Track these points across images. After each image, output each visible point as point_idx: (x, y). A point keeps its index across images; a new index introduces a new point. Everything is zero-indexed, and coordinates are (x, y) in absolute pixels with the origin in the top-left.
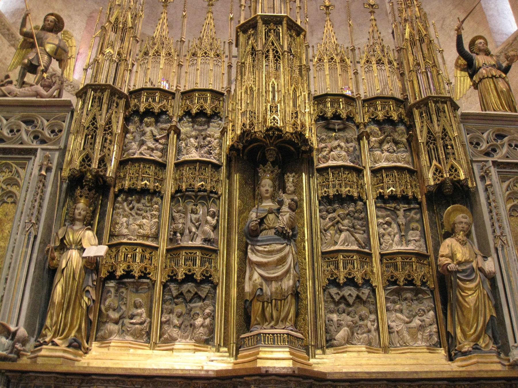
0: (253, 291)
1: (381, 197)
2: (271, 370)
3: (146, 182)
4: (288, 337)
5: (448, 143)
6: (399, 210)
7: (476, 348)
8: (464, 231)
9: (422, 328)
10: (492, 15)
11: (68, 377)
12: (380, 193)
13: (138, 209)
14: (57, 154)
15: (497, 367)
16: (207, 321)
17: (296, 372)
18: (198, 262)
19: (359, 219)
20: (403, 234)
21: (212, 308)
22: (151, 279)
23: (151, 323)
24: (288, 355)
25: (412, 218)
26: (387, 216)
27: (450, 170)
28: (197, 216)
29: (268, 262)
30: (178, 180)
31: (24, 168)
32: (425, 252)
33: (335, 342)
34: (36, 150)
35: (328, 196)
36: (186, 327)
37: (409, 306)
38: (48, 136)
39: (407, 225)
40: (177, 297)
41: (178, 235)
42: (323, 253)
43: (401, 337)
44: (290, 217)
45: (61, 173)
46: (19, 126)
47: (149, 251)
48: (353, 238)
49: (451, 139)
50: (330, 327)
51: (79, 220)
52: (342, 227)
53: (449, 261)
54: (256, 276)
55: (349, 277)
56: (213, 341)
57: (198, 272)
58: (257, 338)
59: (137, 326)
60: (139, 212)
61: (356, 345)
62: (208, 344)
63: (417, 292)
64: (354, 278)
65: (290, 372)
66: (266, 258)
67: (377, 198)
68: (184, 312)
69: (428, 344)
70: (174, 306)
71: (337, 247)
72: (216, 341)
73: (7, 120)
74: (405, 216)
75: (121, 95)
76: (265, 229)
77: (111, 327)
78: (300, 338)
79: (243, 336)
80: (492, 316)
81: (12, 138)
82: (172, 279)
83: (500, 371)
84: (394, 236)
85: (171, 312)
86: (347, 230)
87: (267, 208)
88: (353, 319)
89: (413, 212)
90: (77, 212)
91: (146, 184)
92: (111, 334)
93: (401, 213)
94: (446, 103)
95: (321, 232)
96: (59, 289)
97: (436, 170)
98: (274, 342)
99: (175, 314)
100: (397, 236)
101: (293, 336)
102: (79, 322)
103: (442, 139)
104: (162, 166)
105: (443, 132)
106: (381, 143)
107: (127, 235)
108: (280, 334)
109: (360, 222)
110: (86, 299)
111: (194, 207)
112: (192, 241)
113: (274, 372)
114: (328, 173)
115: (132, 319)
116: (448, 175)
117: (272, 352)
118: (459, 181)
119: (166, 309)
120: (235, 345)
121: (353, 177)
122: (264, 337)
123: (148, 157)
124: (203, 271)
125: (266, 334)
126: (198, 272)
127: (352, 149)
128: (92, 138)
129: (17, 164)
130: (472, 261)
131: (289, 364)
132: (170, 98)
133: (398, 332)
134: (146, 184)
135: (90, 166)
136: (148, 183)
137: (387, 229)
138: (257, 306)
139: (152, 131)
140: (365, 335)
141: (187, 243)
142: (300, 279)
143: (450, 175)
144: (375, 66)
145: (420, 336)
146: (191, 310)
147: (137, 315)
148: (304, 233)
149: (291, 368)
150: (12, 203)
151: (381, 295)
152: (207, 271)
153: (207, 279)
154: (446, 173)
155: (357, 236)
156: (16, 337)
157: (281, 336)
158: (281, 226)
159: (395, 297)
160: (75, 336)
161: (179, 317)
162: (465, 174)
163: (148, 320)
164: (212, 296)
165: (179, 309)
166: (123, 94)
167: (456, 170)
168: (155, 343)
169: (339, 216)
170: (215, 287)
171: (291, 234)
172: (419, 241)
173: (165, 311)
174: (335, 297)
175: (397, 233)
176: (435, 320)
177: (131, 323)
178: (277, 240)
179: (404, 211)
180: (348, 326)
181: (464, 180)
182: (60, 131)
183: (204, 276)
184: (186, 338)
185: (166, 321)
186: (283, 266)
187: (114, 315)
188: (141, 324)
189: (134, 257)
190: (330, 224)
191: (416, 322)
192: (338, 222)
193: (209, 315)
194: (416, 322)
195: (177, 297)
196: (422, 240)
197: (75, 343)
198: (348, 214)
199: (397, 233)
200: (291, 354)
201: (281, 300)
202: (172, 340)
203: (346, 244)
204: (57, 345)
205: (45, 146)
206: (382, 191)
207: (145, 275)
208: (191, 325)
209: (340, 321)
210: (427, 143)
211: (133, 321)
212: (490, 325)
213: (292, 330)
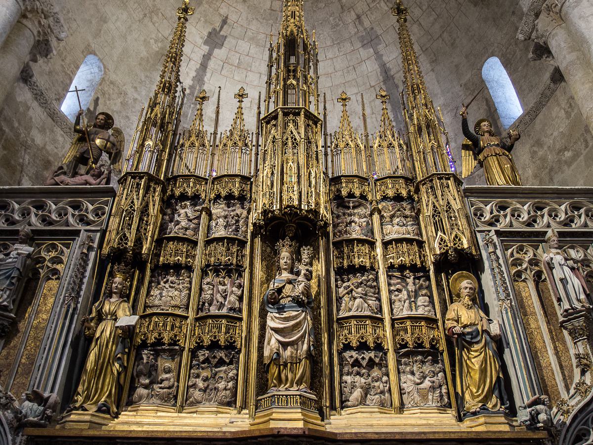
0: (270, 355)
2: (282, 430)
3: (179, 257)
4: (300, 398)
5: (452, 215)
6: (409, 278)
7: (484, 409)
8: (469, 296)
9: (433, 388)
10: (500, 102)
11: (94, 441)
12: (391, 263)
13: (172, 283)
14: (99, 234)
15: (506, 428)
16: (230, 385)
17: (307, 433)
18: (223, 329)
19: (371, 287)
20: (413, 299)
21: (235, 371)
22: (180, 346)
23: (178, 386)
24: (299, 416)
25: (422, 285)
26: (398, 284)
27: (454, 239)
28: (224, 288)
29: (285, 328)
31: (68, 248)
32: (434, 317)
33: (349, 403)
34: (80, 231)
35: (343, 266)
36: (211, 390)
37: (419, 367)
38: (93, 219)
40: (203, 362)
41: (206, 304)
42: (338, 319)
43: (412, 397)
44: (305, 286)
45: (100, 252)
46: (66, 209)
47: (179, 320)
48: (366, 305)
49: (454, 211)
50: (345, 389)
51: (115, 293)
52: (356, 295)
53: (455, 324)
54: (273, 341)
55: (362, 341)
56: (235, 404)
58: (271, 400)
59: (165, 390)
60: (172, 285)
61: (369, 405)
62: (231, 406)
64: (366, 342)
65: (301, 432)
66: (282, 324)
67: (389, 268)
68: (209, 376)
69: (439, 404)
70: (201, 370)
71: (351, 314)
72: (238, 404)
73: (56, 205)
74: (414, 284)
75: (158, 182)
76: (283, 298)
77: (141, 391)
78: (312, 400)
79: (259, 398)
80: (498, 378)
81: (60, 221)
82: (199, 347)
83: (508, 432)
84: (405, 302)
85: (198, 376)
86: (361, 297)
87: (285, 279)
88: (367, 381)
89: (422, 279)
90: (114, 285)
91: (179, 259)
92: (140, 398)
93: (410, 281)
94: (450, 179)
95: (337, 300)
96: (92, 357)
97: (442, 240)
98: (287, 403)
99: (201, 378)
100: (407, 301)
101: (305, 397)
102: (109, 388)
103: (447, 211)
105: (447, 206)
106: (392, 217)
107: (159, 306)
108: (293, 395)
109: (372, 290)
110: (117, 365)
111: (221, 279)
112: (219, 310)
113: (285, 433)
114: (343, 247)
115: (161, 384)
116: (452, 245)
117: (285, 413)
118: (463, 249)
119: (193, 373)
120: (254, 406)
121: (366, 249)
122: (278, 399)
123: (181, 235)
124: (228, 338)
125: (279, 395)
127: (365, 223)
128: (129, 219)
129: (63, 244)
130: (477, 324)
131: (300, 425)
132: (203, 183)
133: (409, 393)
134: (179, 259)
135: (126, 244)
136: (181, 259)
137: (398, 295)
138: (274, 370)
139: (186, 212)
140: (377, 396)
143: (455, 244)
144: (385, 149)
145: (430, 397)
146: (216, 374)
147: (167, 379)
148: (320, 300)
149: (301, 428)
150: (56, 279)
151: (391, 358)
152: (231, 337)
153: (231, 346)
154: (450, 242)
155: (370, 302)
156: (48, 404)
157: (293, 398)
158: (296, 294)
159: (406, 359)
160: (105, 401)
161: (204, 381)
162: (468, 243)
163: (176, 384)
164: (234, 361)
165: (204, 374)
166: (160, 180)
167: (460, 240)
168: (182, 406)
169: (353, 284)
171: (306, 301)
172: (428, 306)
173: (192, 375)
174: (349, 360)
175: (407, 299)
176: (445, 381)
177: (161, 388)
178: (293, 307)
179: (414, 279)
180: (362, 388)
181: (467, 248)
182: (103, 214)
183: (229, 342)
184: (210, 401)
185: (193, 385)
186: (299, 331)
188: (169, 388)
189: (165, 325)
190: (344, 292)
191: (427, 383)
192: (352, 290)
193: (232, 379)
194: (427, 383)
195: (203, 362)
196: (431, 305)
197: (104, 408)
198: (361, 283)
199: (407, 299)
200: (303, 415)
201: (296, 363)
202: (198, 402)
203: (360, 310)
204: (86, 410)
205: (88, 228)
206: (392, 261)
207: (174, 342)
208: (215, 388)
209: (354, 382)
210: (433, 216)
211: (162, 385)
212: (497, 386)
213: (305, 392)
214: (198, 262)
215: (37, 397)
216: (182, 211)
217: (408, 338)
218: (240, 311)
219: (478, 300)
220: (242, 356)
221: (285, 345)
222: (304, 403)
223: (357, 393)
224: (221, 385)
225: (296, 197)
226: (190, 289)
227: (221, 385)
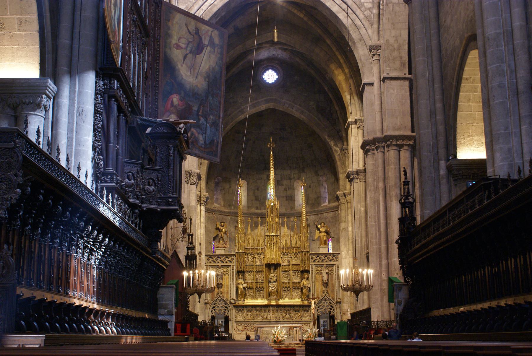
9: (298, 295)
15: (307, 303)
30: (256, 268)
39: (298, 276)
57: (261, 286)
63: (298, 288)
82: (257, 287)
93: (297, 273)
126: (261, 286)
131: (275, 303)
141: (259, 281)
142: (277, 289)
153: (262, 287)
165: (258, 293)
170: (264, 289)
187: (248, 294)
194: (297, 294)
215: (233, 299)
216: (249, 257)
219: (308, 279)
221: (272, 289)
222: (276, 299)
223: (285, 296)
224: (262, 295)
225: (274, 261)
226: (253, 276)
227: (262, 295)
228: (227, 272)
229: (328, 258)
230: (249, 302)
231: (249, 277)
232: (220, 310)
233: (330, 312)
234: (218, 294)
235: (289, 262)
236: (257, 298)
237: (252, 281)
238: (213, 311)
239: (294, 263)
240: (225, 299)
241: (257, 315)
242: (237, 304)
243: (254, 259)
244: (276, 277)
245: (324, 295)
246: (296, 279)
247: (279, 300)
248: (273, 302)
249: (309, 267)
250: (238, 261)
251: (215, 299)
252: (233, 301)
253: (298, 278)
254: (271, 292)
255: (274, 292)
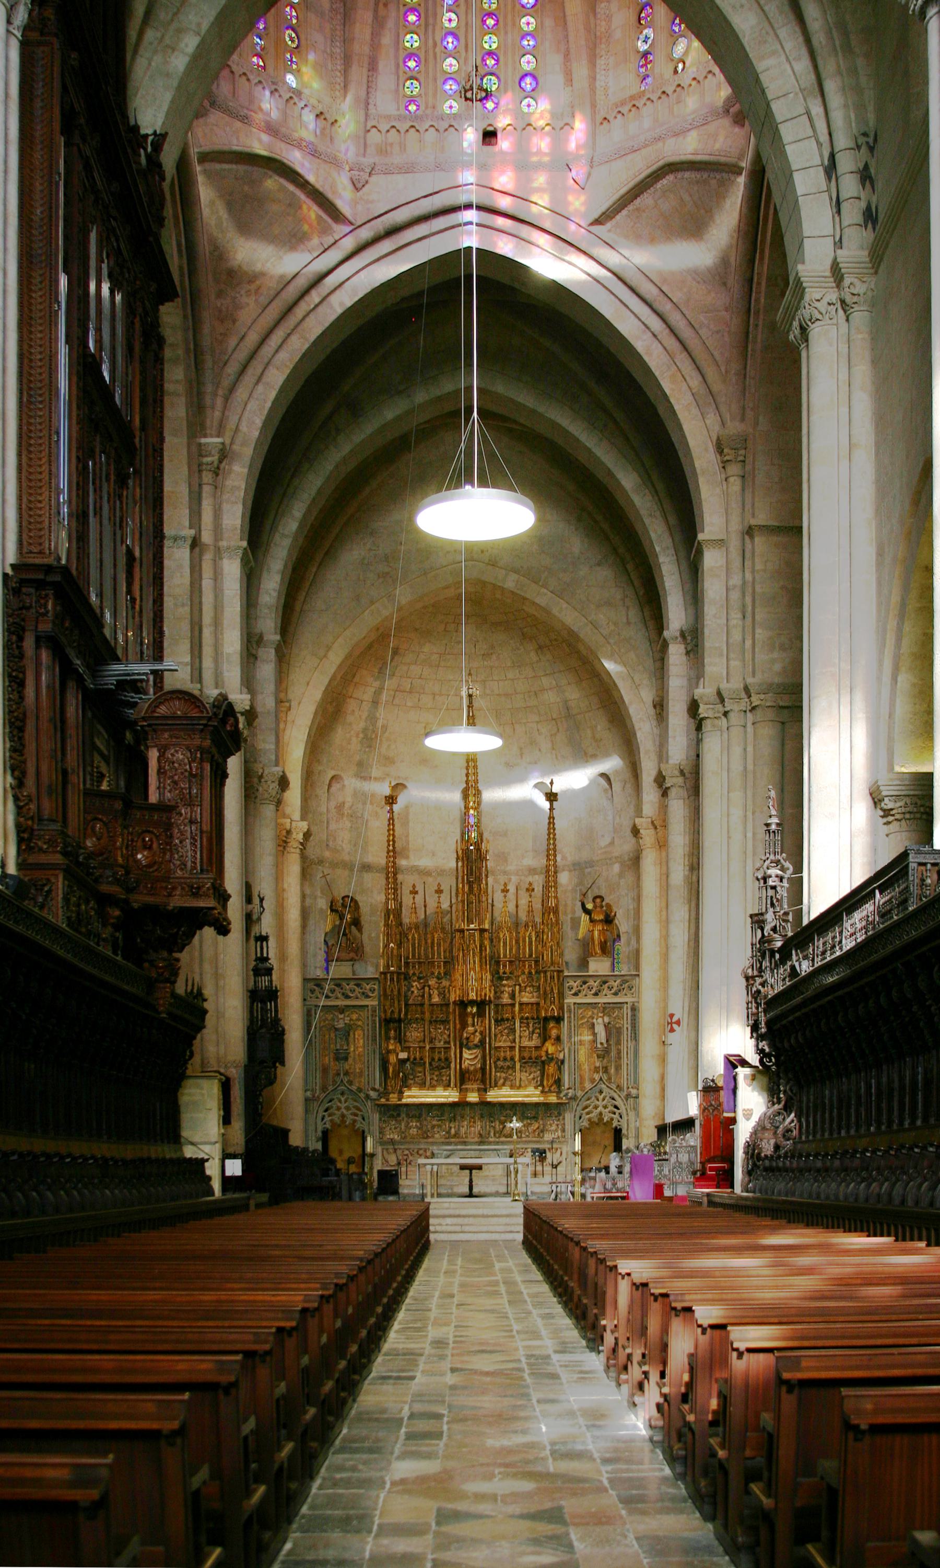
1: (522, 1018)
30: (432, 1013)
104: (422, 1005)
141: (438, 1045)
151: (518, 1066)
164: (449, 1067)
207: (421, 1059)
214: (427, 1016)
217: (526, 1055)
218: (449, 1043)
219: (558, 1039)
220: (453, 1065)
223: (502, 1081)
228: (360, 1023)
229: (610, 988)
230: (415, 1096)
231: (414, 1034)
232: (343, 1116)
233: (612, 1119)
234: (338, 1074)
235: (513, 996)
236: (433, 1087)
237: (422, 1044)
238: (327, 1119)
239: (525, 1000)
240: (354, 1088)
241: (433, 1127)
242: (383, 1100)
243: (427, 989)
244: (481, 1033)
245: (597, 1077)
246: (527, 1039)
247: (485, 1090)
248: (473, 1097)
249: (561, 1008)
250: (385, 995)
251: (331, 1088)
252: (373, 1094)
253: (535, 1036)
254: (468, 1071)
255: (476, 1071)
